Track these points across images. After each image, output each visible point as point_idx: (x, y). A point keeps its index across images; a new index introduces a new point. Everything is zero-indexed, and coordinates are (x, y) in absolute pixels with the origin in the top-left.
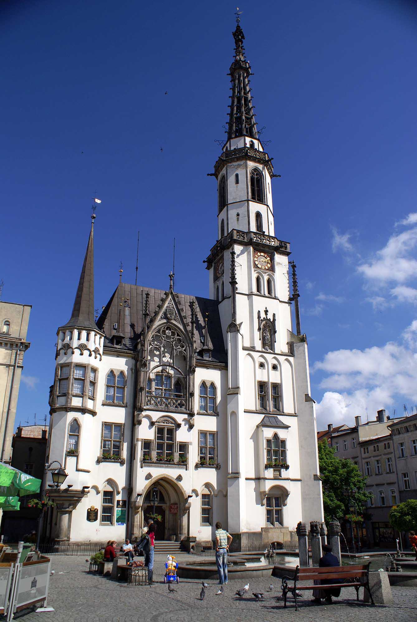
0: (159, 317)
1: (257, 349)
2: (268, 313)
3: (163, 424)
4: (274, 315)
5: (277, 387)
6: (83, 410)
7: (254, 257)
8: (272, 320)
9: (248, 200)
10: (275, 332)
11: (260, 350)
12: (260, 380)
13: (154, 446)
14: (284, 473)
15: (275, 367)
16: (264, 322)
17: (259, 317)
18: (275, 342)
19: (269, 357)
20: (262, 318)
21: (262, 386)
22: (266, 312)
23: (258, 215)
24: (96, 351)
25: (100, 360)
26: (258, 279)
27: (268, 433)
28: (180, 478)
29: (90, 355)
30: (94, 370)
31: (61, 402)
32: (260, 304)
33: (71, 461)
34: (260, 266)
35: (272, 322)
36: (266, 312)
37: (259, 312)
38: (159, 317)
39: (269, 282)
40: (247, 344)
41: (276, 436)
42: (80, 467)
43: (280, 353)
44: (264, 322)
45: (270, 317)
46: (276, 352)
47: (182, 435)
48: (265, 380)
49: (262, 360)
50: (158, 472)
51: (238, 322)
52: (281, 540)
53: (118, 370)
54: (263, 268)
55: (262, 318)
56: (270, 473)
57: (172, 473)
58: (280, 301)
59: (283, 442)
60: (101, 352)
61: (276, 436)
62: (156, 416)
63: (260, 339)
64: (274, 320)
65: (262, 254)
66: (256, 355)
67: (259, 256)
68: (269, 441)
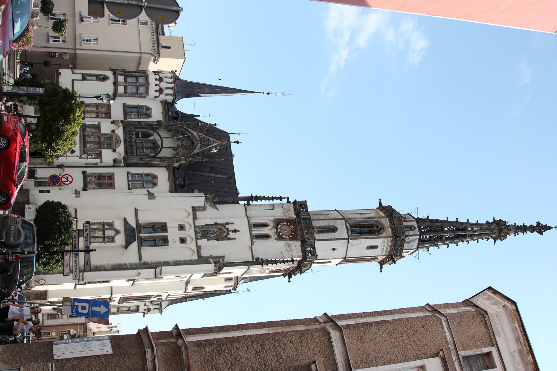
0: (199, 134)
1: (196, 221)
2: (234, 233)
3: (114, 139)
4: (235, 239)
5: (165, 241)
6: (116, 83)
8: (229, 236)
9: (344, 219)
10: (217, 240)
11: (196, 225)
12: (168, 225)
15: (183, 240)
16: (225, 230)
17: (228, 224)
20: (227, 226)
21: (163, 227)
22: (235, 231)
23: (334, 229)
25: (156, 97)
26: (265, 225)
27: (119, 225)
29: (156, 85)
30: (147, 93)
31: (121, 79)
33: (80, 77)
34: (279, 227)
35: (226, 236)
36: (235, 231)
37: (233, 223)
39: (267, 237)
40: (198, 214)
41: (118, 232)
42: (75, 82)
43: (199, 244)
44: (225, 230)
45: (231, 235)
46: (198, 241)
48: (169, 230)
49: (187, 227)
51: (218, 206)
54: (279, 231)
55: (227, 226)
60: (163, 97)
62: (120, 132)
63: (206, 224)
64: (229, 239)
65: (293, 230)
66: (190, 219)
67: (289, 226)
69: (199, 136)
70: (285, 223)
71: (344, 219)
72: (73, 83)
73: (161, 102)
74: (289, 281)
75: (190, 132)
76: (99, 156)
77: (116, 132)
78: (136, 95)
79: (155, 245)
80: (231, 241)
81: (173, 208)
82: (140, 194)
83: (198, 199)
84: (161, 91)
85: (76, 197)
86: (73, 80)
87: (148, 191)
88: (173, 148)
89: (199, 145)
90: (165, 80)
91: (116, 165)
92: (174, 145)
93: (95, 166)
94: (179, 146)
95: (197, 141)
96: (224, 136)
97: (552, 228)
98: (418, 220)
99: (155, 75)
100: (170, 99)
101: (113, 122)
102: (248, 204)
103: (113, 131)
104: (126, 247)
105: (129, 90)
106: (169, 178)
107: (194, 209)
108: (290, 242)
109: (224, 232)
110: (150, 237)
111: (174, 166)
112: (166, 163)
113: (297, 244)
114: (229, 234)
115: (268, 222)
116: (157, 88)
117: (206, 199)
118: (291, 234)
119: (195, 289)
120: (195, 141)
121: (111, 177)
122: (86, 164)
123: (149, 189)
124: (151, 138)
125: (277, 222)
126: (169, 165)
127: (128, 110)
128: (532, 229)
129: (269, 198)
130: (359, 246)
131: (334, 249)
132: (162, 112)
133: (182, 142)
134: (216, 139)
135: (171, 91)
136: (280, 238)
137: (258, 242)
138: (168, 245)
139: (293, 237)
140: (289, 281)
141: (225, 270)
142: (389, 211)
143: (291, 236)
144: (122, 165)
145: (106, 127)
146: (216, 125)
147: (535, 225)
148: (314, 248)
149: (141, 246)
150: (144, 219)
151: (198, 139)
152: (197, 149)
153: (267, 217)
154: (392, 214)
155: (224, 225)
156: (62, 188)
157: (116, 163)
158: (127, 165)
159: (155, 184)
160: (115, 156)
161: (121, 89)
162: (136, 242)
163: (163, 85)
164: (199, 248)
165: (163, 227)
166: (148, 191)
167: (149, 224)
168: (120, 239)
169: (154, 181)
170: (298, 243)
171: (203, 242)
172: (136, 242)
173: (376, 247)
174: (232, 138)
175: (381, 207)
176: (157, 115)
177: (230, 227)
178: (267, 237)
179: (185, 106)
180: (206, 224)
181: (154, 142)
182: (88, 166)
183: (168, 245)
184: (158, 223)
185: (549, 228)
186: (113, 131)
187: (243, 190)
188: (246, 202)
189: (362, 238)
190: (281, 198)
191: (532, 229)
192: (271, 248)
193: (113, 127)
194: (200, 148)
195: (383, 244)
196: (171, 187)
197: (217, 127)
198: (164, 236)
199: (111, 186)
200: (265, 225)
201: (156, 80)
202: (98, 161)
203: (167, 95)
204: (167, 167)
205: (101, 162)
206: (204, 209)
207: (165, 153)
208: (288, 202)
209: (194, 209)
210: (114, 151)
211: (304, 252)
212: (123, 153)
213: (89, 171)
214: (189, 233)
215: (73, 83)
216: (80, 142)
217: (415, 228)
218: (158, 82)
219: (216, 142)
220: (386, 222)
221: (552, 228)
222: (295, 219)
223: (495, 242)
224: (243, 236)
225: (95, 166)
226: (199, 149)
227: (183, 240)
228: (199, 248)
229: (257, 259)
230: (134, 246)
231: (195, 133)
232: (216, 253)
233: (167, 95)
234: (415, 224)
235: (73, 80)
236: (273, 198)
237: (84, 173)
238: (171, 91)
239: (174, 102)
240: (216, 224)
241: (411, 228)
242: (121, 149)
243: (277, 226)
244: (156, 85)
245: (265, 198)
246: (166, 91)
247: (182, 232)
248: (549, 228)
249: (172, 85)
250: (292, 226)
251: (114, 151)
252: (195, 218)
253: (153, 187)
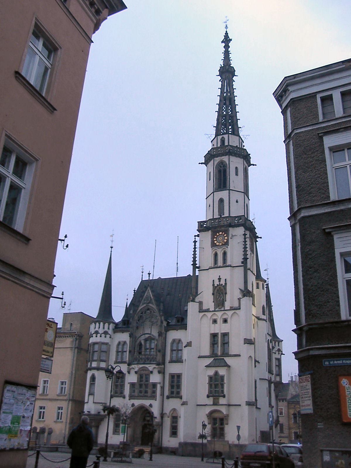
6: (98, 369)
7: (213, 238)
10: (226, 293)
12: (213, 332)
13: (137, 386)
14: (222, 401)
15: (225, 321)
17: (213, 285)
18: (226, 301)
19: (219, 314)
20: (216, 285)
21: (214, 336)
22: (220, 279)
23: (221, 201)
24: (106, 333)
25: (110, 337)
26: (216, 255)
28: (151, 405)
30: (107, 344)
31: (94, 364)
32: (214, 274)
33: (91, 397)
34: (217, 244)
36: (220, 279)
39: (225, 254)
40: (205, 307)
41: (216, 373)
43: (229, 308)
45: (223, 282)
47: (155, 378)
49: (215, 317)
50: (137, 402)
52: (221, 451)
53: (123, 341)
54: (221, 244)
55: (216, 285)
56: (210, 401)
57: (146, 403)
58: (234, 267)
59: (222, 377)
60: (110, 332)
61: (216, 373)
63: (213, 302)
64: (226, 284)
65: (221, 233)
66: (209, 315)
68: (211, 378)
70: (215, 239)
71: (213, 192)
72: (96, 403)
73: (114, 333)
74: (261, 238)
76: (154, 385)
77: (136, 370)
78: (107, 352)
79: (228, 343)
80: (227, 282)
81: (198, 329)
82: (186, 353)
83: (192, 308)
84: (106, 333)
85: (187, 404)
86: (94, 403)
87: (185, 347)
90: (97, 329)
91: (163, 371)
93: (163, 388)
95: (146, 306)
96: (145, 285)
97: (226, 31)
98: (217, 135)
99: (92, 337)
100: (112, 326)
101: (129, 372)
102: (198, 268)
103: (136, 372)
104: (229, 366)
105: (104, 358)
106: (175, 329)
107: (201, 311)
108: (230, 236)
109: (220, 288)
110: (221, 346)
111: (166, 325)
112: (163, 331)
113: (232, 231)
114: (222, 284)
115: (214, 253)
116: (103, 335)
117: (193, 301)
118: (224, 235)
119: (264, 314)
121: (172, 376)
122: (161, 395)
123: (184, 346)
124: (143, 342)
125: (213, 245)
126: (165, 330)
127: (119, 360)
128: (227, 47)
129: (195, 251)
130: (235, 181)
131: (237, 202)
134: (146, 290)
135: (106, 325)
136: (227, 244)
137: (228, 263)
138: (228, 333)
139: (226, 232)
140: (261, 238)
141: (250, 289)
142: (209, 157)
143: (225, 235)
144: (163, 366)
145: (132, 378)
146: (134, 291)
147: (224, 44)
148: (236, 217)
149: (229, 354)
150: (206, 350)
151: (145, 305)
152: (153, 306)
153: (209, 252)
154: (211, 155)
155: (214, 287)
156: (179, 416)
157: (162, 372)
158: (164, 363)
159: (180, 340)
160: (156, 372)
161: (103, 365)
162: (225, 358)
163: (101, 331)
164: (232, 309)
165: (214, 336)
166: (185, 347)
167: (211, 347)
168: (222, 371)
169: (177, 341)
170: (230, 229)
171: (227, 305)
172: (225, 358)
173: (236, 168)
174: (146, 278)
175: (206, 163)
176: (125, 337)
177: (217, 283)
178: (225, 254)
179: (118, 314)
180: (213, 302)
181: (146, 340)
182: (162, 394)
183: (228, 333)
184: (211, 339)
185: (226, 33)
186: (136, 372)
187: (186, 271)
188: (197, 270)
189: (229, 179)
190: (195, 242)
191: (227, 47)
192: (235, 251)
193: (133, 372)
194: (152, 303)
195: (235, 163)
196: (181, 329)
197: (136, 290)
198: (221, 336)
199: (179, 376)
200: (216, 255)
201: (96, 337)
202: (159, 386)
203: (109, 328)
205: (160, 383)
206: (201, 303)
207: (155, 333)
208: (198, 236)
209: (201, 311)
210: (152, 372)
211: (238, 226)
212: (154, 366)
213: (167, 393)
214: (219, 315)
215: (96, 403)
216: (144, 399)
217: (223, 137)
218: (99, 335)
219: (149, 291)
220: (217, 160)
221: (226, 31)
222: (212, 231)
223: (236, 76)
224: (224, 273)
225: (163, 388)
226: (153, 305)
227: (225, 321)
228: (232, 309)
229: (242, 263)
230: (228, 360)
231: (140, 308)
232: (238, 294)
233: (109, 328)
234: (220, 137)
235: (94, 403)
236: (195, 248)
237: (168, 397)
238: (106, 325)
239: (114, 323)
240: (213, 294)
241: (223, 141)
242: (151, 367)
243: (217, 245)
244: (101, 336)
245: (195, 254)
246: (106, 329)
247: (218, 321)
248: (226, 33)
249: (102, 324)
250: (218, 234)
251: (152, 372)
252: (208, 311)
253: (182, 343)
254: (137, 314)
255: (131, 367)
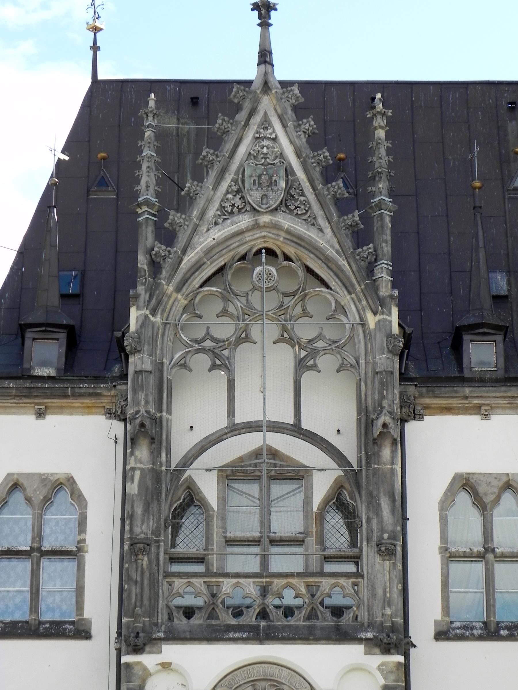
0: (212, 212)
38: (212, 212)
69: (226, 213)
75: (198, 266)
88: (302, 366)
89: (286, 221)
92: (282, 360)
94: (286, 337)
95: (256, 226)
106: (476, 410)
120: (256, 241)
132: (40, 415)
133: (259, 316)
152: (312, 234)
204: (410, 412)
212: (352, 653)
219: (266, 124)
226: (313, 223)
254: (184, 281)
255: (148, 660)
